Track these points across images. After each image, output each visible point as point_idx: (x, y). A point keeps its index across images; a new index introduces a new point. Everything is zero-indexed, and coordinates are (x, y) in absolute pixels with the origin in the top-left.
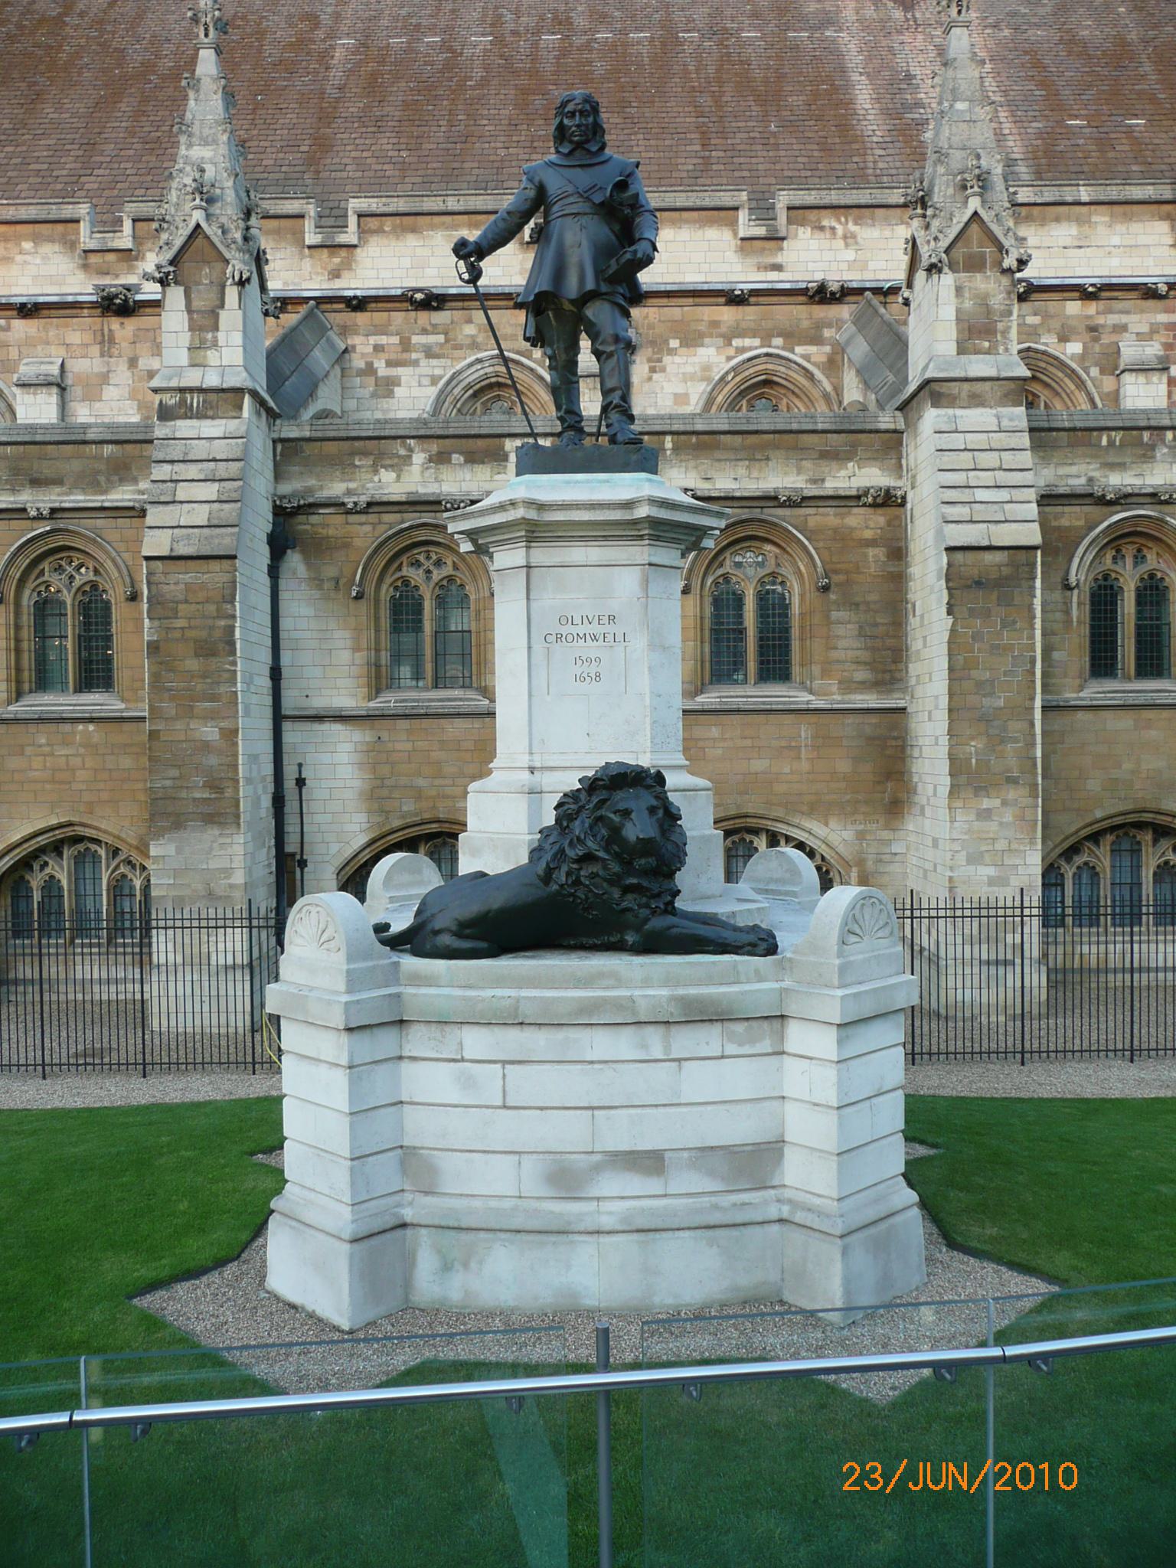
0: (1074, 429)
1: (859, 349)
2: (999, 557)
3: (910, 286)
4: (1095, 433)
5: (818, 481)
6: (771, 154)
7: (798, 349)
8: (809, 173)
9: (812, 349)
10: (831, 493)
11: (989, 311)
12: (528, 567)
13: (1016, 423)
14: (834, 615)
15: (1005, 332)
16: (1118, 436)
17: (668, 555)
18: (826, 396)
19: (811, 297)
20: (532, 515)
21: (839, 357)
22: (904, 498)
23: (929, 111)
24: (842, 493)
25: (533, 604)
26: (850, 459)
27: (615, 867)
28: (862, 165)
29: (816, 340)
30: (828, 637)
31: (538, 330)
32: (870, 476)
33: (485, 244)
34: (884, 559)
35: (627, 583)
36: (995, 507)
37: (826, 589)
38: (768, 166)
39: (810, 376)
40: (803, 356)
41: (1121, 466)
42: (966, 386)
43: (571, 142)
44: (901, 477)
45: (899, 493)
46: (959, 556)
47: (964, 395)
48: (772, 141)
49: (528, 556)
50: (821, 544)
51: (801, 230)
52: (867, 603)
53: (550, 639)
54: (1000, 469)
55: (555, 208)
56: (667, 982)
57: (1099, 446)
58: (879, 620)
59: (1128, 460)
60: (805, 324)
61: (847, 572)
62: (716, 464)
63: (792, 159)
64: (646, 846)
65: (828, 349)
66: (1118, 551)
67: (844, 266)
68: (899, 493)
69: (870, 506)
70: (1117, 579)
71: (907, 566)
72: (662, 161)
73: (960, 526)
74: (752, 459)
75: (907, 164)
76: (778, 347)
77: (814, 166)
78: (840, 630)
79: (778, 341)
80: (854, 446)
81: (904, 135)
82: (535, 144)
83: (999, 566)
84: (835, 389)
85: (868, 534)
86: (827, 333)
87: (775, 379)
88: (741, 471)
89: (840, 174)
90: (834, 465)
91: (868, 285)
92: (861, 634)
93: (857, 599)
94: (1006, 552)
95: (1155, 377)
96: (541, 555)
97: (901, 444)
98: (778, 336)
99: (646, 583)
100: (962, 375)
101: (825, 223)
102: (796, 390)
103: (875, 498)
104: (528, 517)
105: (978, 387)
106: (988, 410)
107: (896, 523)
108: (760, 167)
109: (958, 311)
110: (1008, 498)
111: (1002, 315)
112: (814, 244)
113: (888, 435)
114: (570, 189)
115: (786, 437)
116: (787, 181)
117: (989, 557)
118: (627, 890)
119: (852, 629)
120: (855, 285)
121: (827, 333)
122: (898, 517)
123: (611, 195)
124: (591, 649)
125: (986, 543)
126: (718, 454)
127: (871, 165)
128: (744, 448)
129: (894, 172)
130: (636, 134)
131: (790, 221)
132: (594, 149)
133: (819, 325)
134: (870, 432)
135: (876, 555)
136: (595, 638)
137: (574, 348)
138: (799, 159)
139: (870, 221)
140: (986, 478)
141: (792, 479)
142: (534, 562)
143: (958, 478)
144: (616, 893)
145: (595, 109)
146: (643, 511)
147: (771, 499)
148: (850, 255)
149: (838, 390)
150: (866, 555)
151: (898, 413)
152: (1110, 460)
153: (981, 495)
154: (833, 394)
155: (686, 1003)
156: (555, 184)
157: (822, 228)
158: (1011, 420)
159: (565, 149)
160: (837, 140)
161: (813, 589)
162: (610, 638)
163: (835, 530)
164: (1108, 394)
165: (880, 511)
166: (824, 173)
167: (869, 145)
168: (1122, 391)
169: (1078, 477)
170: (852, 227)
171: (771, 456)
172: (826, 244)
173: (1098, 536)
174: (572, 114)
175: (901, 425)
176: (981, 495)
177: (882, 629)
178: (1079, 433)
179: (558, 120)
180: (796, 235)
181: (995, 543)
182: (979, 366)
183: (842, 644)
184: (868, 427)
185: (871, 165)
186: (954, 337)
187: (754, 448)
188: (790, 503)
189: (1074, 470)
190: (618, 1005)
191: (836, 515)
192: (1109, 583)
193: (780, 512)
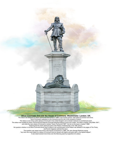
20: (52, 55)
27: (59, 82)
31: (53, 39)
56: (63, 90)
64: (61, 81)
96: (53, 59)
99: (63, 61)
118: (60, 84)
124: (58, 68)
132: (59, 22)
144: (59, 84)
145: (59, 19)
146: (63, 55)
155: (64, 91)
190: (60, 92)
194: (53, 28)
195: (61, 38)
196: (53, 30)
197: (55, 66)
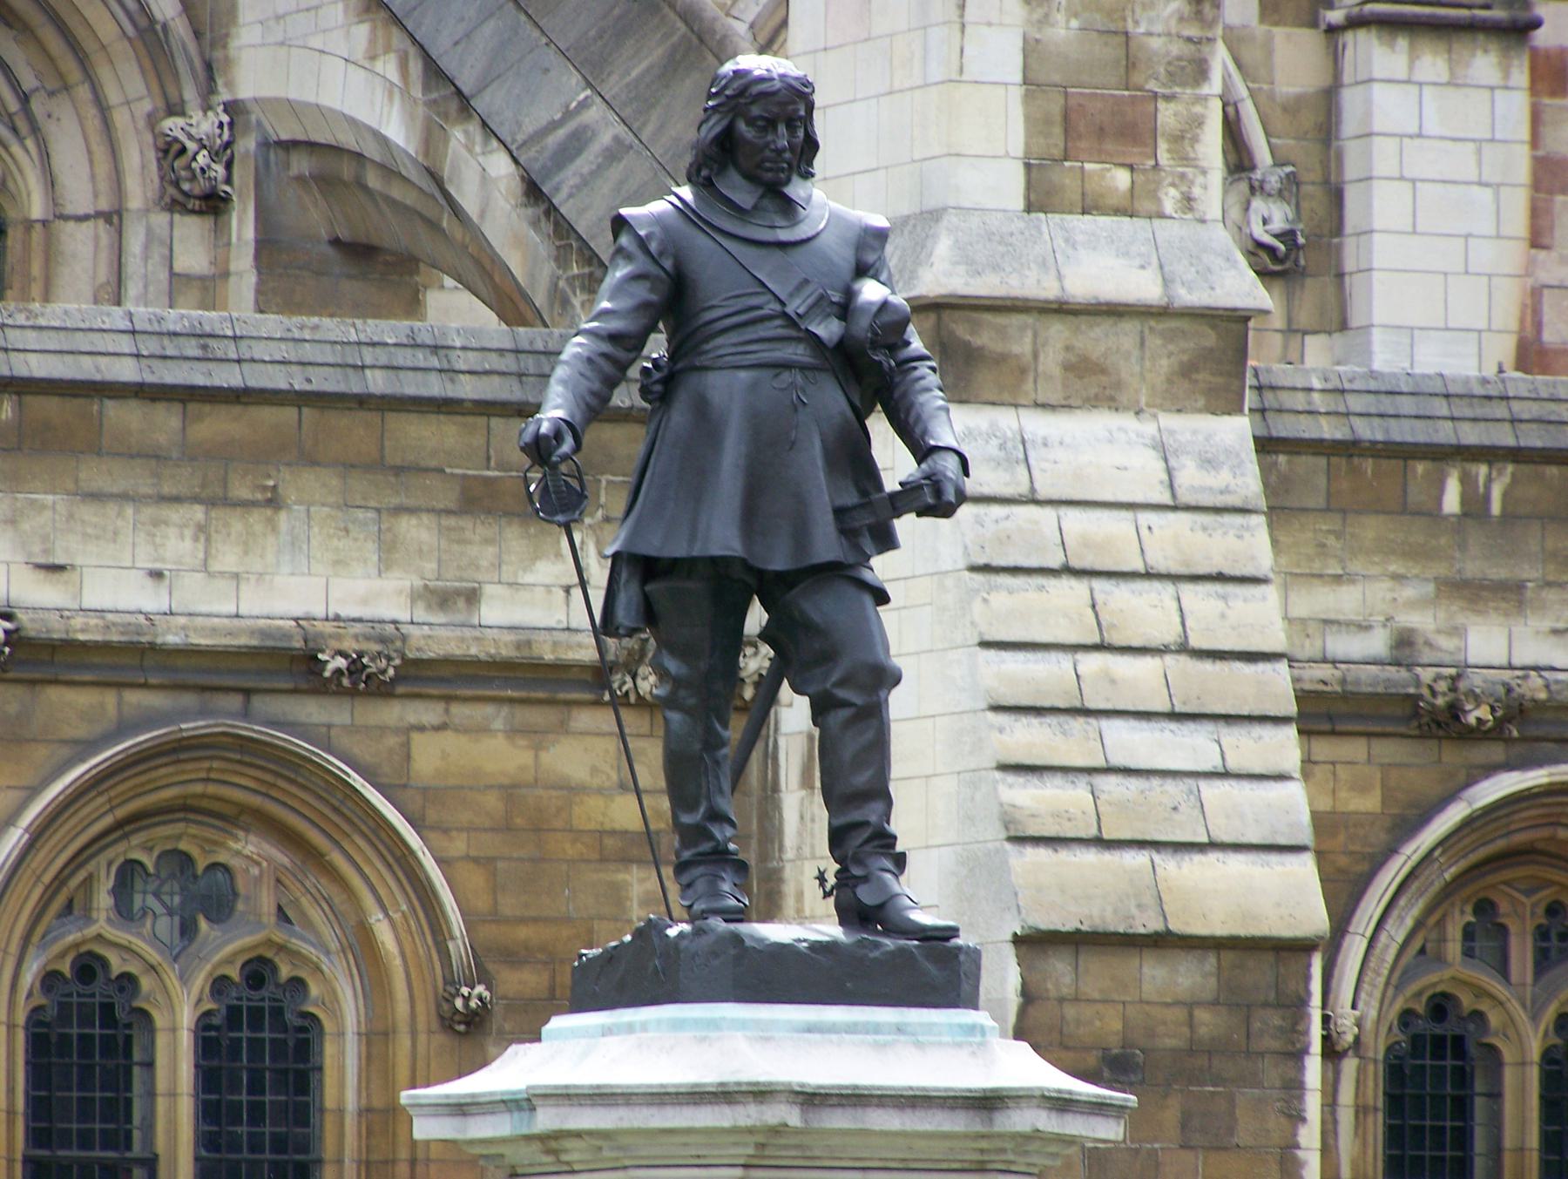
0: (1348, 449)
2: (1187, 977)
4: (1420, 468)
5: (457, 598)
11: (1130, 59)
13: (1223, 478)
15: (1185, 137)
16: (1498, 486)
36: (1173, 788)
41: (1508, 595)
42: (1057, 332)
46: (1059, 970)
47: (1051, 361)
50: (458, 846)
54: (1184, 649)
57: (1433, 513)
59: (1529, 572)
62: (88, 512)
66: (1485, 908)
70: (1478, 1016)
73: (1065, 855)
74: (217, 501)
83: (1190, 1005)
88: (177, 543)
94: (1211, 960)
95: (1484, 63)
100: (1048, 290)
105: (1098, 339)
106: (1127, 421)
109: (1031, 50)
110: (1212, 762)
111: (1172, 77)
115: (340, 420)
117: (1159, 977)
125: (1154, 925)
126: (95, 474)
128: (192, 454)
140: (1141, 679)
143: (1044, 676)
147: (292, 663)
152: (1473, 568)
153: (1130, 742)
158: (1208, 463)
161: (425, 1015)
163: (510, 791)
164: (1293, 107)
168: (1350, 99)
169: (1364, 627)
171: (290, 494)
173: (1428, 857)
176: (1130, 742)
178: (1369, 465)
179: (715, 126)
181: (1176, 926)
182: (1102, 262)
186: (1015, 139)
187: (223, 455)
188: (361, 681)
189: (1345, 601)
191: (513, 732)
192: (1448, 1029)
193: (312, 710)
195: (868, 600)
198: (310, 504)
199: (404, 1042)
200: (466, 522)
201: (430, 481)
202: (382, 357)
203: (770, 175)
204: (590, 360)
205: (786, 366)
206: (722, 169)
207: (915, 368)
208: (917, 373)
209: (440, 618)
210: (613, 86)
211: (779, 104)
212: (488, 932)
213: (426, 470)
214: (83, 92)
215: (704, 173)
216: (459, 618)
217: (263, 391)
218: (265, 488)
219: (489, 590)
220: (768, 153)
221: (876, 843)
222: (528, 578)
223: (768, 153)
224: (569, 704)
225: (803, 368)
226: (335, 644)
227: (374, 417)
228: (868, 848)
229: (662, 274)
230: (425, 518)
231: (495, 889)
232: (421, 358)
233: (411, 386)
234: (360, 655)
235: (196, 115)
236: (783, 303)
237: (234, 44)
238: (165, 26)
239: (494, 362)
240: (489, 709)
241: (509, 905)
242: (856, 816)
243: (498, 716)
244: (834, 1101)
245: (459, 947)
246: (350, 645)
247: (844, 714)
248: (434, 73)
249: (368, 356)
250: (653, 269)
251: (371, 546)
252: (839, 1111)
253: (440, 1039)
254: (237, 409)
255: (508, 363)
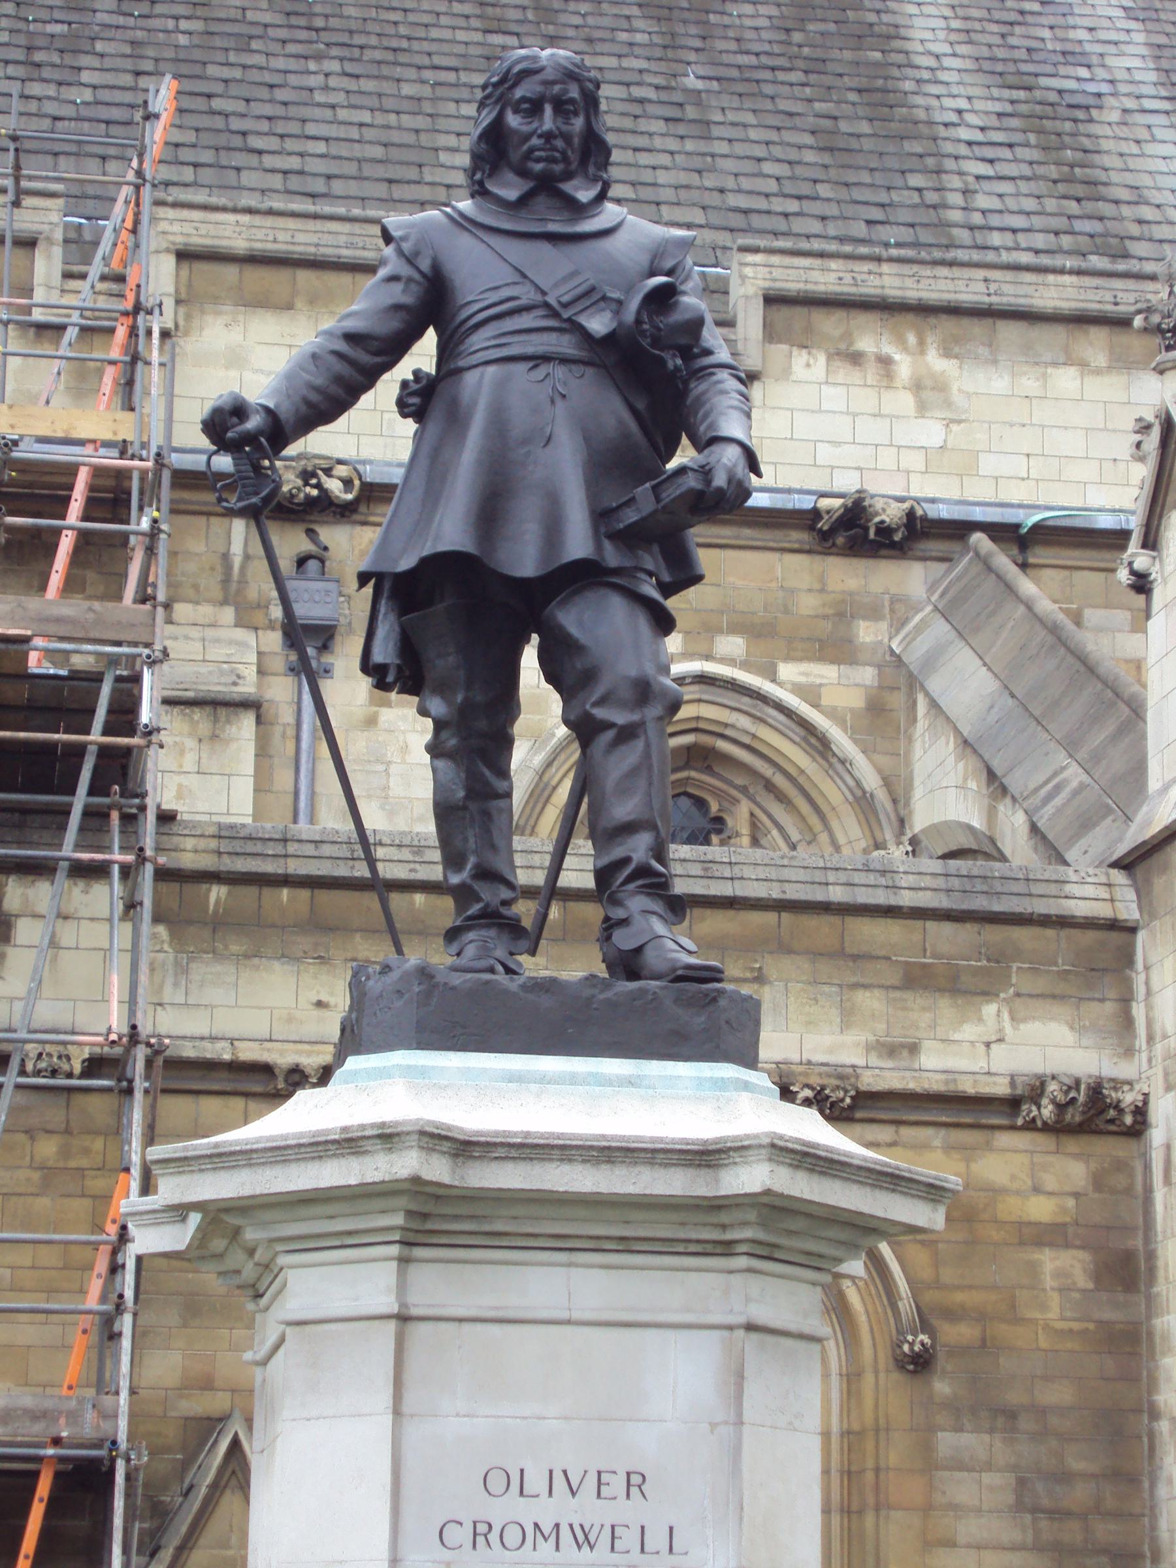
1: (966, 683)
3: (1151, 541)
6: (689, 146)
7: (788, 671)
8: (793, 206)
9: (825, 673)
10: (935, 1084)
12: (403, 1318)
14: (947, 1442)
17: (787, 1301)
18: (863, 802)
19: (825, 536)
20: (438, 1170)
21: (897, 700)
22: (1141, 1112)
23: (1101, 73)
24: (968, 1087)
25: (413, 1432)
26: (988, 994)
28: (932, 197)
29: (835, 647)
30: (928, 1509)
31: (408, 647)
32: (1043, 1044)
33: (286, 413)
34: (1083, 1281)
35: (679, 1377)
37: (919, 1364)
38: (683, 178)
39: (819, 744)
40: (798, 689)
43: (523, 173)
44: (1129, 1052)
45: (1129, 1098)
48: (691, 112)
49: (402, 1286)
51: (800, 359)
52: (1041, 1412)
53: (451, 1533)
55: (478, 340)
58: (1076, 1465)
60: (808, 604)
61: (981, 1317)
63: (748, 167)
65: (867, 675)
67: (915, 461)
68: (1129, 1098)
69: (1047, 1128)
71: (1152, 1306)
72: (395, 137)
75: (1051, 204)
76: (730, 661)
77: (805, 189)
78: (962, 1489)
79: (733, 644)
80: (1000, 958)
81: (1040, 132)
82: (39, 57)
84: (887, 783)
85: (1041, 1209)
86: (867, 633)
87: (723, 745)
89: (877, 214)
90: (944, 1004)
91: (978, 514)
92: (1023, 1503)
93: (1014, 1397)
96: (441, 1285)
97: (1127, 958)
98: (734, 629)
101: (866, 344)
102: (779, 780)
103: (1061, 1108)
104: (427, 1175)
107: (1121, 1181)
108: (662, 177)
112: (834, 397)
113: (1090, 936)
114: (527, 295)
116: (737, 221)
119: (996, 1486)
120: (944, 512)
121: (867, 633)
122: (1121, 1166)
123: (638, 321)
127: (956, 199)
129: (1019, 222)
130: (319, 57)
131: (770, 334)
133: (845, 612)
134: (1045, 921)
135: (1063, 1267)
136: (583, 1539)
137: (504, 700)
138: (768, 168)
139: (983, 351)
141: (828, 1040)
142: (419, 1304)
145: (591, 102)
146: (750, 1178)
148: (931, 433)
149: (898, 789)
150: (1033, 1268)
151: (1119, 877)
154: (882, 796)
156: (482, 272)
157: (855, 359)
159: (510, 189)
160: (865, 127)
162: (628, 1539)
165: (1072, 1144)
166: (832, 210)
167: (948, 148)
170: (935, 361)
171: (771, 972)
172: (865, 399)
174: (534, 107)
175: (1128, 909)
177: (1080, 1495)
180: (787, 372)
183: (969, 1529)
184: (1041, 907)
185: (956, 199)
191: (948, 1148)
194: (423, 355)
196: (419, 400)
197: (503, 1510)
198: (787, 981)
199: (869, 1378)
200: (908, 995)
201: (880, 965)
202: (843, 877)
203: (538, 167)
204: (314, 356)
205: (545, 358)
206: (494, 171)
207: (713, 374)
208: (715, 378)
209: (889, 1064)
210: (1082, 754)
211: (546, 83)
212: (930, 1297)
213: (878, 958)
214: (824, 838)
215: (478, 176)
216: (903, 1064)
217: (745, 899)
218: (752, 969)
219: (926, 1044)
220: (535, 141)
221: (640, 882)
222: (957, 1036)
223: (535, 141)
224: (993, 1128)
225: (564, 360)
226: (805, 1081)
227: (835, 920)
228: (631, 886)
229: (417, 276)
230: (877, 992)
231: (936, 1263)
232: (871, 879)
233: (864, 897)
234: (823, 1088)
235: (892, 848)
236: (544, 293)
237: (913, 801)
238: (872, 795)
239: (927, 881)
240: (929, 1131)
241: (948, 1275)
242: (618, 853)
243: (936, 1137)
244: (501, 1152)
245: (906, 1304)
246: (815, 1081)
247: (610, 735)
248: (991, 775)
249: (831, 877)
250: (405, 270)
251: (835, 1012)
252: (509, 1166)
253: (896, 1375)
254: (731, 913)
255: (940, 882)
